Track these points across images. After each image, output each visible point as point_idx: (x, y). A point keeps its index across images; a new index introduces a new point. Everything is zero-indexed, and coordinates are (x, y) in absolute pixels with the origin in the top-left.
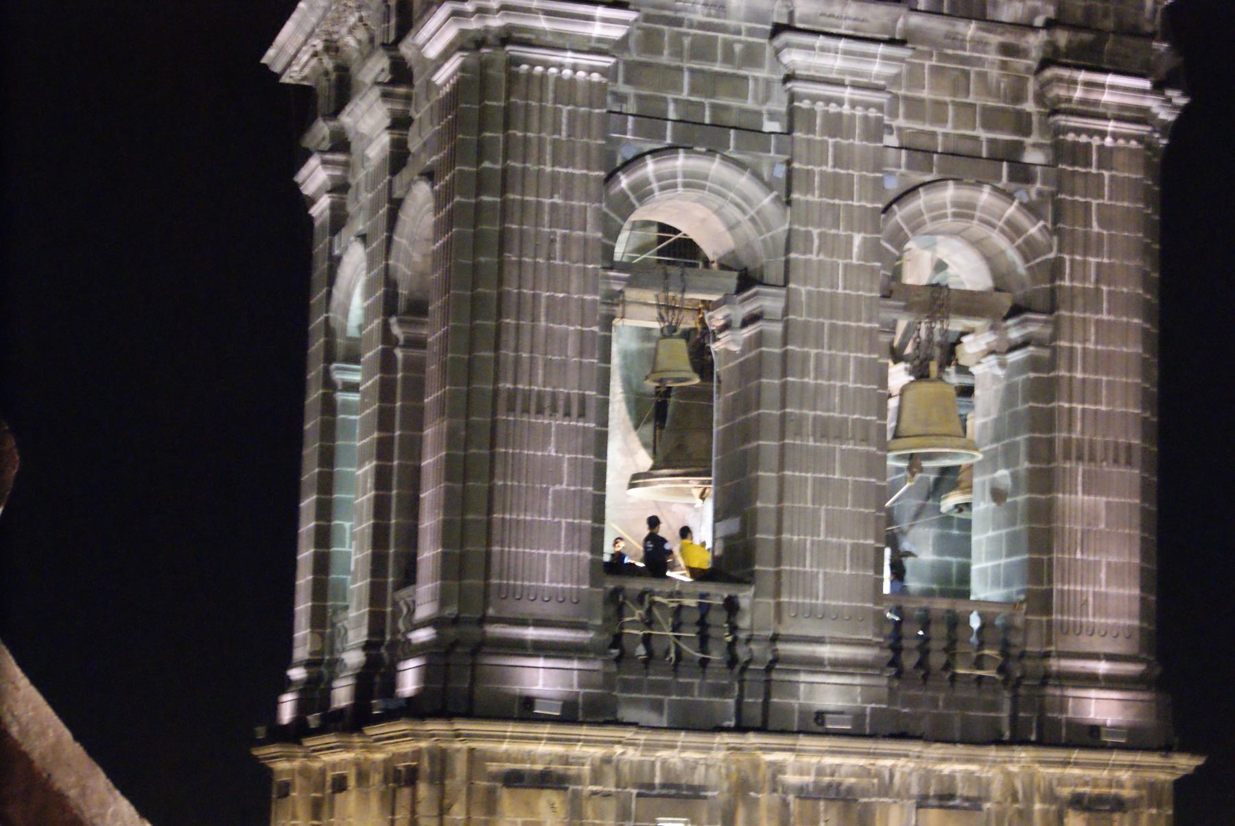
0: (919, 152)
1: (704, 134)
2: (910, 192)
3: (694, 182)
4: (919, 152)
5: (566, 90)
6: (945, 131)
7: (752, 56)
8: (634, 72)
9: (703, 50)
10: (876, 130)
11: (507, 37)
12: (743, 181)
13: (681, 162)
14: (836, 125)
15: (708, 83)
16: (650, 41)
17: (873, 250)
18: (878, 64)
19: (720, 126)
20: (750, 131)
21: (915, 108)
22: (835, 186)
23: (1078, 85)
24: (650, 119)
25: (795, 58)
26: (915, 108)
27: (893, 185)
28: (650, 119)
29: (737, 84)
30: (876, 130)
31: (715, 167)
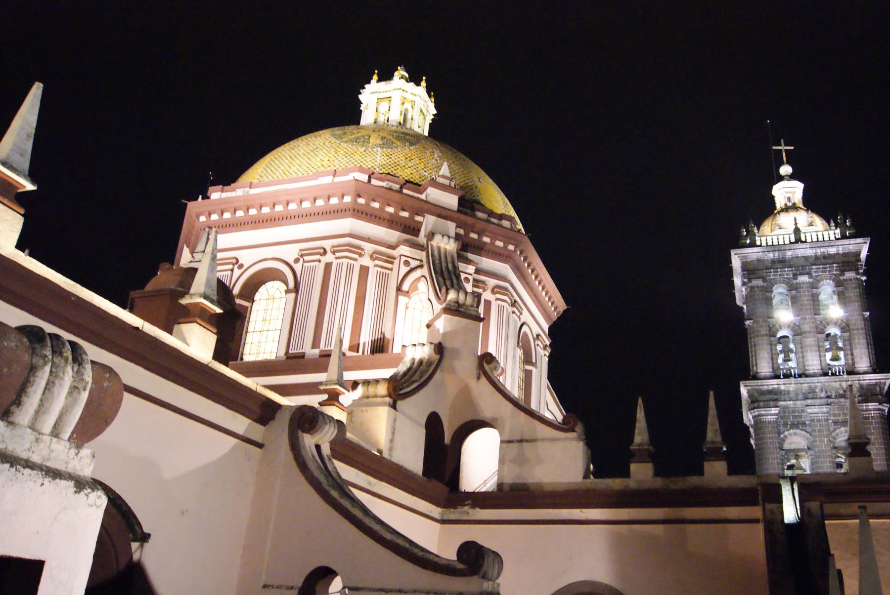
0: (836, 423)
1: (794, 426)
2: (835, 430)
3: (795, 434)
4: (836, 423)
5: (770, 422)
6: (841, 418)
7: (803, 411)
8: (782, 418)
9: (794, 412)
10: (827, 420)
11: (759, 415)
12: (803, 432)
13: (792, 431)
14: (819, 420)
15: (794, 417)
16: (784, 412)
17: (829, 441)
18: (825, 409)
19: (798, 424)
20: (804, 424)
21: (835, 415)
22: (820, 431)
23: (864, 406)
24: (785, 425)
25: (809, 411)
26: (835, 415)
27: (832, 429)
28: (785, 425)
29: (800, 416)
30: (827, 420)
31: (798, 431)
